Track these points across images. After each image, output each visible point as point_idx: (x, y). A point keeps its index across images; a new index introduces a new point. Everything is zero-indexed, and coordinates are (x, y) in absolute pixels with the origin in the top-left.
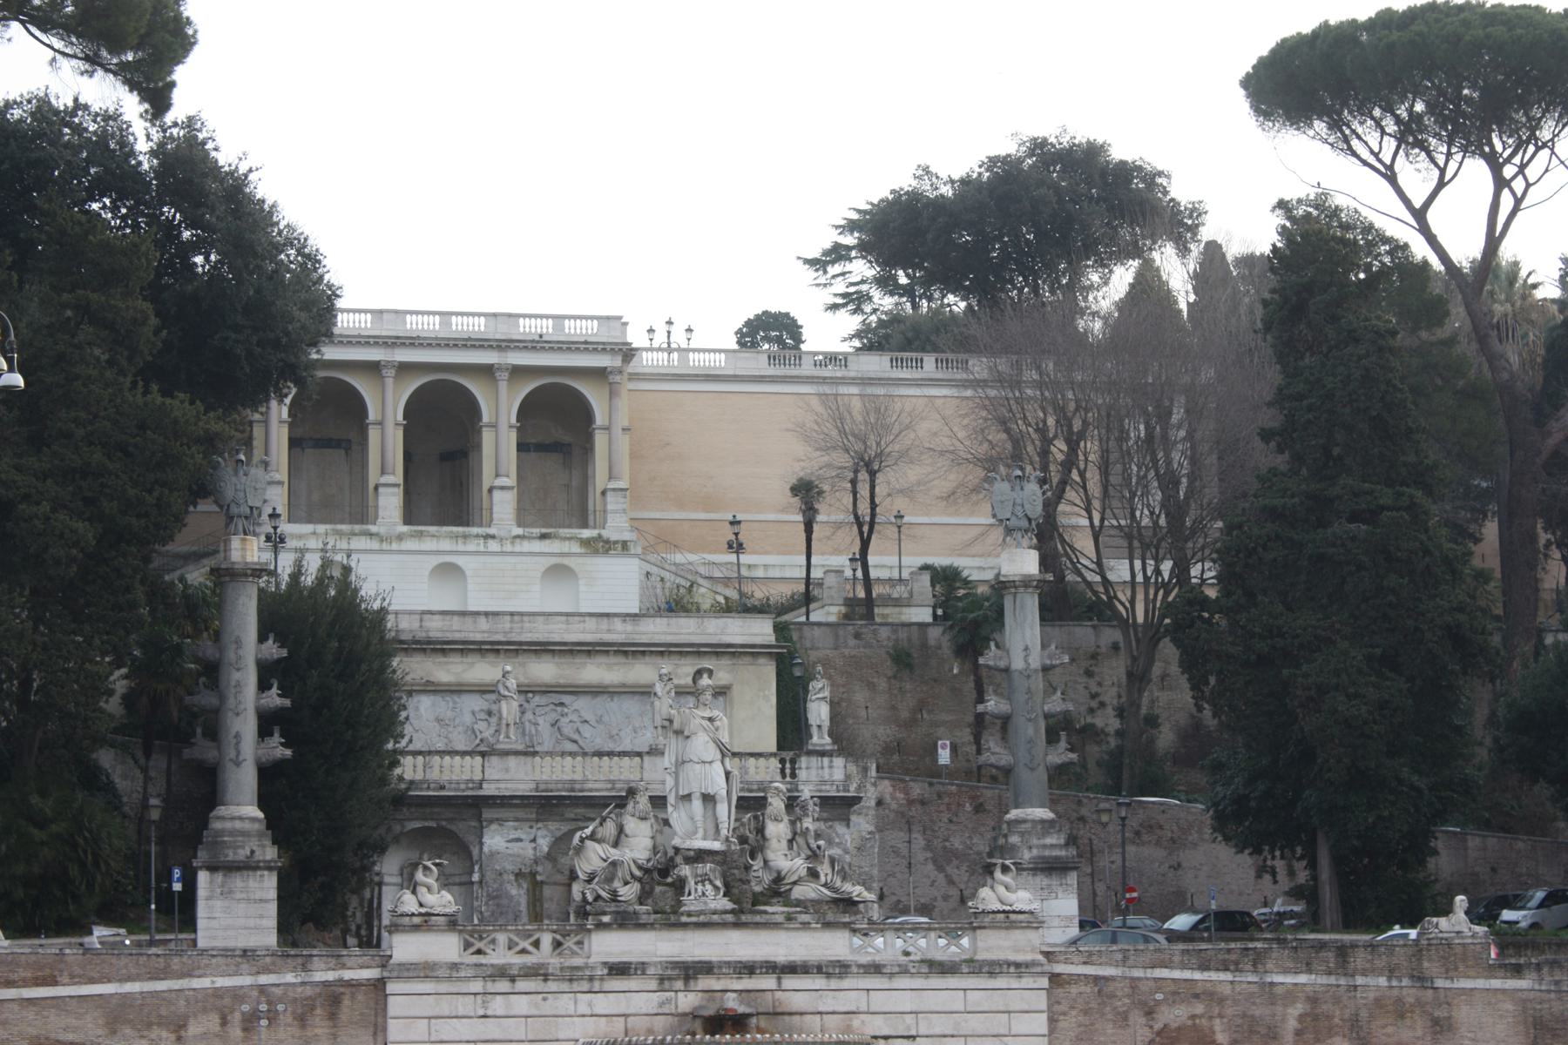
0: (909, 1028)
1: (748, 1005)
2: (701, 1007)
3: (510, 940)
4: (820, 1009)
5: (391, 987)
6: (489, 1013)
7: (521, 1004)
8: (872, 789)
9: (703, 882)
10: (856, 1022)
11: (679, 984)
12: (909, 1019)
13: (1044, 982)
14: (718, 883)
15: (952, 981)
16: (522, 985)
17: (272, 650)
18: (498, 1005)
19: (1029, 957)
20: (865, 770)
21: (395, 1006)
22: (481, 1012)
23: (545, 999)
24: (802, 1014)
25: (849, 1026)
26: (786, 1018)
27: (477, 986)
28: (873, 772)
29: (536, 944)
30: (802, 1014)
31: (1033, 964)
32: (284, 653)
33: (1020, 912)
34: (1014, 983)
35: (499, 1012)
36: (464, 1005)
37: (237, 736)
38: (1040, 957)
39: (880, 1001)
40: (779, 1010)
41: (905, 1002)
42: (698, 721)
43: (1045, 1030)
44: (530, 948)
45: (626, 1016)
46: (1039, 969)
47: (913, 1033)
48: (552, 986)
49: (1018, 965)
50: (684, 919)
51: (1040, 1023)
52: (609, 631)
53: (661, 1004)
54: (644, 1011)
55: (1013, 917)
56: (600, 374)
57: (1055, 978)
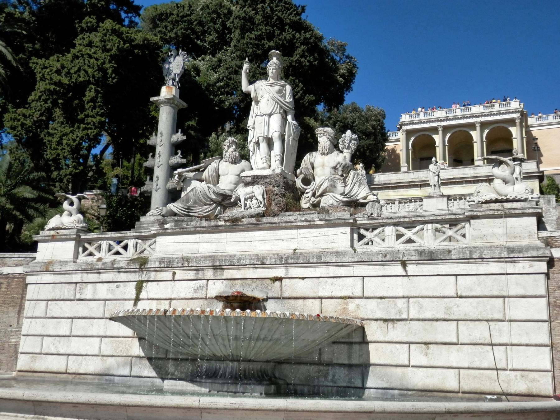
0: (400, 312)
1: (261, 291)
2: (224, 292)
3: (110, 245)
4: (320, 294)
5: (30, 279)
6: (83, 297)
7: (103, 291)
8: (554, 211)
9: (251, 198)
10: (352, 305)
11: (209, 274)
12: (401, 303)
13: (543, 266)
14: (260, 198)
15: (443, 268)
16: (105, 277)
17: (179, 137)
18: (88, 292)
19: (524, 243)
20: (549, 201)
21: (31, 292)
22: (78, 297)
23: (118, 287)
24: (305, 298)
25: (345, 310)
26: (292, 302)
27: (77, 278)
28: (554, 203)
29: (125, 248)
30: (305, 298)
31: (528, 248)
32: (185, 138)
33: (514, 201)
34: (510, 268)
35: (89, 297)
36: (67, 292)
37: (157, 176)
38: (539, 243)
39: (373, 287)
40: (286, 294)
41: (399, 287)
42: (265, 87)
43: (546, 317)
44: (122, 251)
45: (171, 299)
46: (534, 254)
47: (405, 316)
48: (123, 276)
49: (511, 250)
50: (221, 223)
51: (540, 308)
52: (464, 174)
53: (196, 290)
54: (183, 296)
55: (507, 205)
56: (512, 122)
57: (551, 262)
